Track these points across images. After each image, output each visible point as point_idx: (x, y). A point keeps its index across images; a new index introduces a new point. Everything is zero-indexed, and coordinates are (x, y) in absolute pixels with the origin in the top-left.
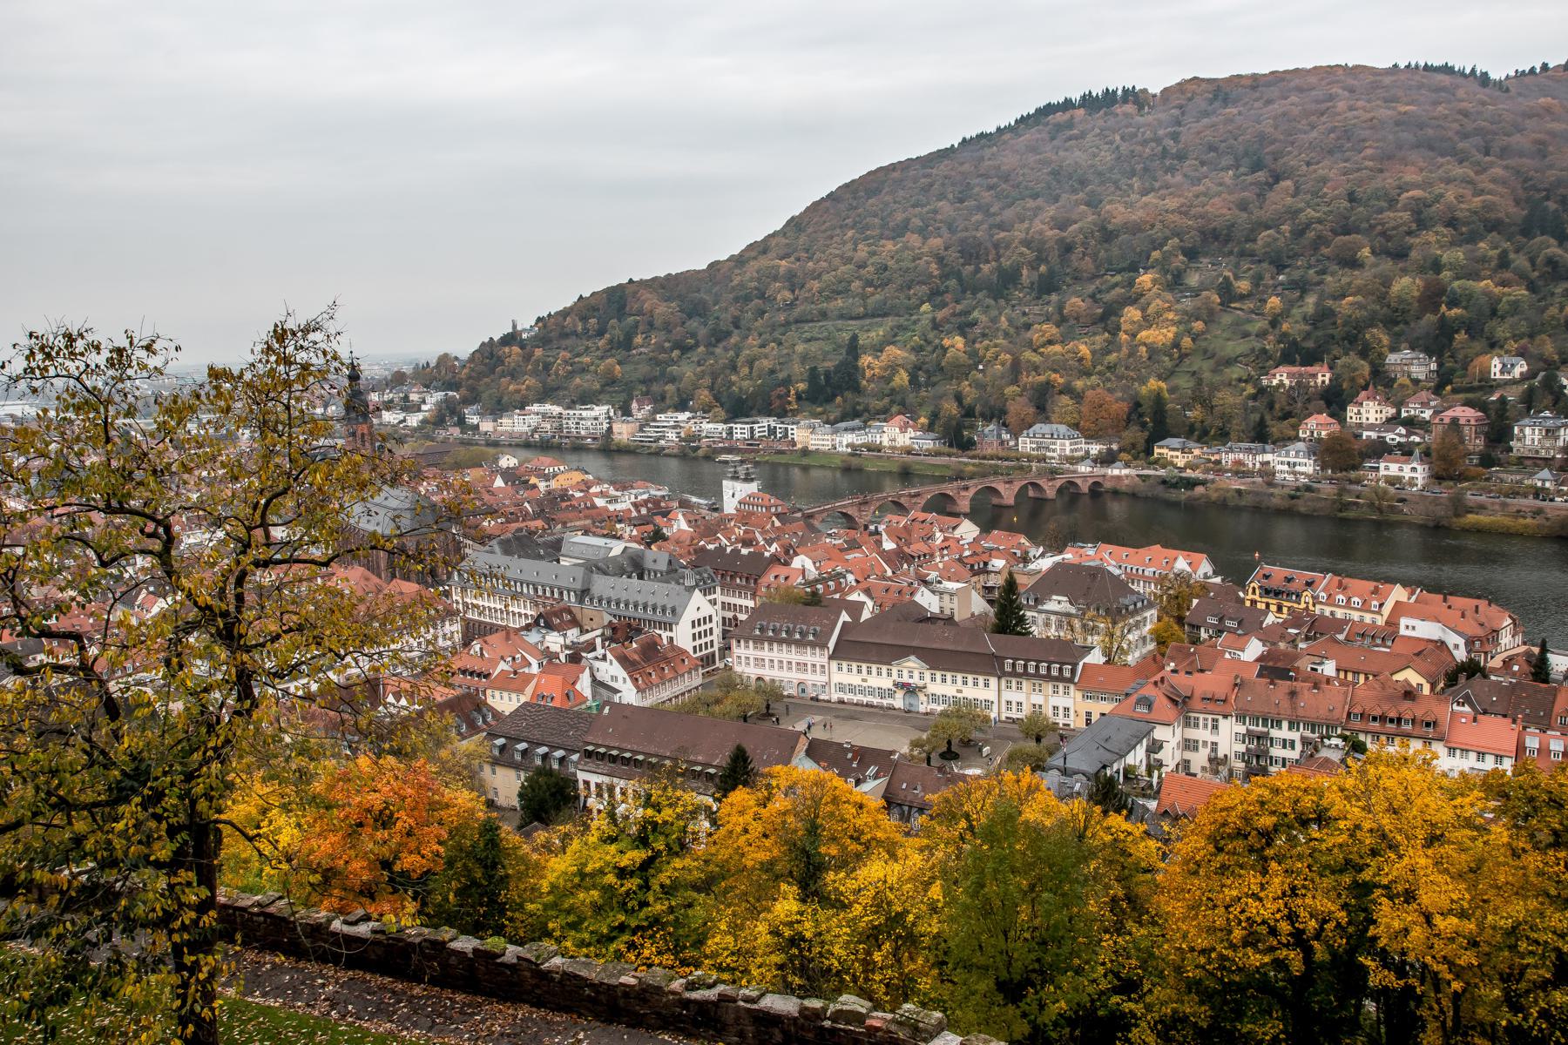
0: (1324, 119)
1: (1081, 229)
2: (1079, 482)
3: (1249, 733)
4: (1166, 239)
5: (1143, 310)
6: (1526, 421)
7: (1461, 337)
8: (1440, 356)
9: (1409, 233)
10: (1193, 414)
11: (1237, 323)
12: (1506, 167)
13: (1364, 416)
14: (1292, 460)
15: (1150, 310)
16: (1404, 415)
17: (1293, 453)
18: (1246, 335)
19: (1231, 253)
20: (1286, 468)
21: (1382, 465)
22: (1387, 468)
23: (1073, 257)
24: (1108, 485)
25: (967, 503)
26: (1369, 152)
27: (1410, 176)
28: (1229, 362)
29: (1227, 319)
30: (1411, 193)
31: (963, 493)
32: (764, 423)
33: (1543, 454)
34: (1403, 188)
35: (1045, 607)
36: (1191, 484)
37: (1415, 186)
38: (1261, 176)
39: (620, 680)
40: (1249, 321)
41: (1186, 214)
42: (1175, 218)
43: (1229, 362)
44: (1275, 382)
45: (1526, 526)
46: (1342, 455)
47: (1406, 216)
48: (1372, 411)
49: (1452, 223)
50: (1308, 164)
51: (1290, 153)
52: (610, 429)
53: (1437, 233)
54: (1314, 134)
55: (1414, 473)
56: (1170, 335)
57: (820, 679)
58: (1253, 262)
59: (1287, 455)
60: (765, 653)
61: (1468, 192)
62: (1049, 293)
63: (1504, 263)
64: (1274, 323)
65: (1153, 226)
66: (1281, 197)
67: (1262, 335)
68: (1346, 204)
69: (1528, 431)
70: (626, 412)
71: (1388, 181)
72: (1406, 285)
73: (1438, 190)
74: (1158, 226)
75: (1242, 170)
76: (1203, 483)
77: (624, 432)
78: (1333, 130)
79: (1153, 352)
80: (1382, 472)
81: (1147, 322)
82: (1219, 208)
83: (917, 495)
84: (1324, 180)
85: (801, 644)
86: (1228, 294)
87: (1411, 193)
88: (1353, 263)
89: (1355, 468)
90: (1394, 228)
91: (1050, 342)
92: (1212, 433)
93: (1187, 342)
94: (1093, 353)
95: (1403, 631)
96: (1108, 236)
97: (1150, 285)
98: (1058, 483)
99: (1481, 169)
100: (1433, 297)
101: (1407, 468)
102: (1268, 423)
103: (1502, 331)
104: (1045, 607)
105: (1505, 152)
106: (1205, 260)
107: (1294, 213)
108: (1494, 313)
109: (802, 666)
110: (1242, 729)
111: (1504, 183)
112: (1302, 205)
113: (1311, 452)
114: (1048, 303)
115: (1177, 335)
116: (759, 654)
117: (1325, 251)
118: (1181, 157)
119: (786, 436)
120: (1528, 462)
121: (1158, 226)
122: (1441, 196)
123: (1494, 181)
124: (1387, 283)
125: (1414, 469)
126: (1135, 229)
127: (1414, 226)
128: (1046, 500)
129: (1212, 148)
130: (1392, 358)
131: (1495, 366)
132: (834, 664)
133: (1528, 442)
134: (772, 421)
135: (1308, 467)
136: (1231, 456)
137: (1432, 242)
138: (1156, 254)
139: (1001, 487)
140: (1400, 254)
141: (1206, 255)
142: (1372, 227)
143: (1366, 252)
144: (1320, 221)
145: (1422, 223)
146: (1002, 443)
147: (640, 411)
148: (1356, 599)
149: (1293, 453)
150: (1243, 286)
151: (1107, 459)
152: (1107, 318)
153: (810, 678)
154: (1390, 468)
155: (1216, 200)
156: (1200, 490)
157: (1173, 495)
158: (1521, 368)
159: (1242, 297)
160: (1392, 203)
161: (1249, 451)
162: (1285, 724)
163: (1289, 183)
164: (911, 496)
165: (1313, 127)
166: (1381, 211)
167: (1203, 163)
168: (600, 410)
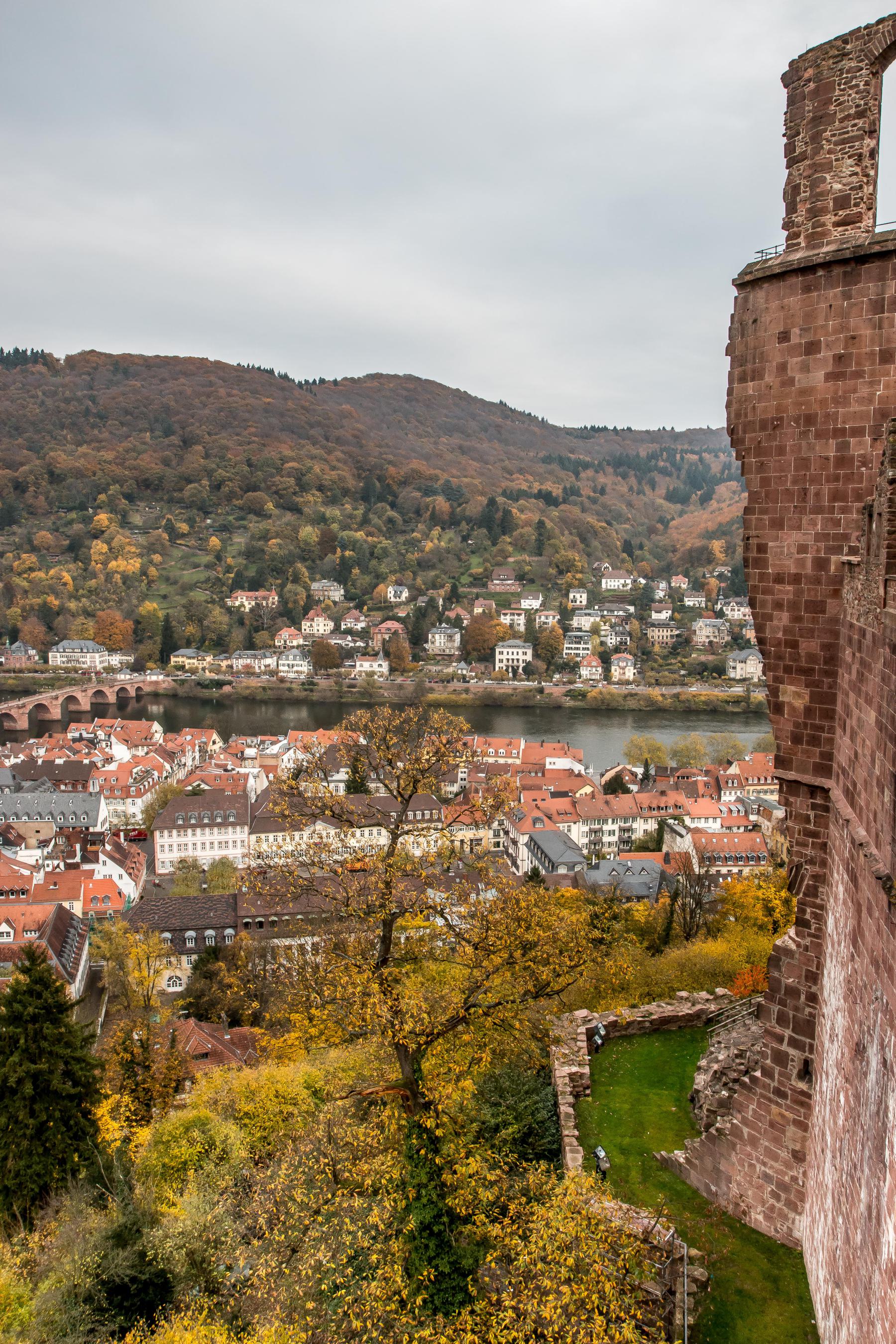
0: (211, 400)
1: (31, 472)
2: (128, 687)
3: (591, 830)
4: (108, 485)
5: (108, 543)
6: (434, 630)
7: (356, 571)
8: (345, 585)
9: (295, 493)
10: (191, 629)
11: (185, 558)
12: (342, 452)
13: (315, 628)
14: (291, 663)
15: (115, 543)
16: (343, 627)
17: (291, 657)
18: (196, 566)
19: (162, 499)
20: (286, 668)
21: (358, 664)
22: (361, 666)
23: (27, 495)
24: (147, 689)
25: (59, 710)
26: (253, 430)
27: (287, 453)
28: (193, 586)
29: (177, 553)
30: (291, 464)
31: (54, 702)
33: (447, 652)
34: (284, 460)
35: (334, 778)
36: (219, 684)
37: (293, 459)
38: (175, 439)
40: (194, 555)
41: (122, 464)
42: (114, 467)
43: (193, 586)
44: (237, 603)
45: (466, 700)
46: (323, 656)
47: (292, 481)
48: (322, 625)
49: (320, 488)
50: (209, 434)
51: (193, 424)
53: (313, 495)
54: (207, 411)
55: (381, 667)
56: (138, 565)
58: (182, 508)
59: (287, 659)
60: (189, 838)
61: (327, 468)
62: (10, 525)
63: (365, 522)
64: (219, 558)
65: (94, 475)
66: (195, 459)
67: (208, 566)
68: (246, 468)
69: (437, 636)
71: (270, 453)
72: (309, 533)
73: (309, 463)
74: (99, 473)
75: (157, 433)
76: (229, 683)
78: (221, 410)
79: (126, 578)
80: (358, 668)
81: (114, 553)
82: (150, 463)
83: (24, 706)
84: (227, 448)
85: (224, 824)
86: (174, 534)
87: (291, 464)
88: (261, 514)
89: (338, 666)
90: (284, 489)
91: (31, 569)
92: (220, 645)
93: (153, 571)
94: (74, 579)
95: (548, 767)
96: (55, 477)
97: (106, 523)
98: (116, 689)
99: (329, 452)
100: (328, 542)
101: (375, 665)
102: (255, 633)
103: (383, 569)
104: (334, 778)
105: (339, 440)
106: (142, 504)
107: (209, 473)
108: (372, 554)
109: (224, 844)
110: (586, 829)
111: (345, 463)
112: (214, 466)
113: (304, 656)
114: (14, 534)
115: (142, 565)
116: (183, 840)
117: (237, 502)
118: (102, 417)
120: (439, 658)
121: (99, 473)
122: (311, 468)
123: (338, 460)
124: (296, 530)
125: (380, 665)
126: (79, 474)
127: (297, 489)
128: (108, 704)
129: (127, 412)
130: (315, 586)
131: (390, 592)
132: (253, 837)
133: (437, 644)
135: (304, 667)
136: (241, 662)
137: (312, 500)
138: (102, 497)
139: (79, 695)
140: (296, 510)
141: (141, 499)
142: (269, 488)
143: (270, 505)
144: (230, 480)
145: (303, 487)
146: (29, 658)
148: (501, 751)
149: (291, 657)
150: (184, 527)
151: (138, 667)
152: (75, 549)
154: (364, 666)
155: (144, 456)
156: (227, 689)
157: (206, 693)
158: (405, 594)
159: (183, 536)
160: (279, 470)
161: (255, 657)
162: (610, 821)
163: (200, 448)
164: (19, 708)
165: (205, 406)
166: (272, 476)
167: (122, 424)
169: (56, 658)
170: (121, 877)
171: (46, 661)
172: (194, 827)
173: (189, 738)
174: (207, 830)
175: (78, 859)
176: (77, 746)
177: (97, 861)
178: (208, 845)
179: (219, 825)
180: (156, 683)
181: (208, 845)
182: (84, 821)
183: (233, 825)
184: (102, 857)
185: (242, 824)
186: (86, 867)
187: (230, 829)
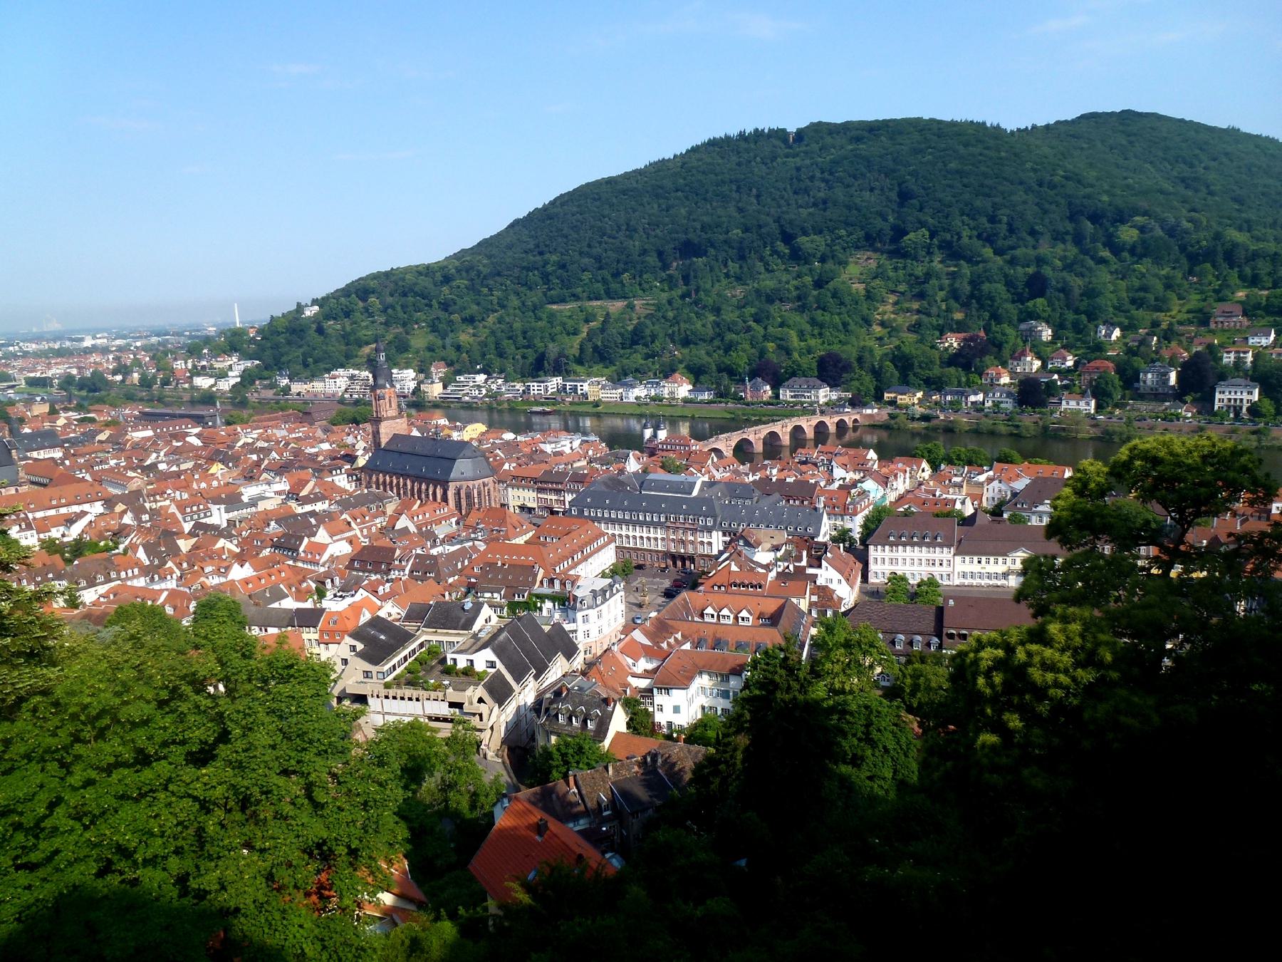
32: (555, 383)
39: (835, 581)
52: (417, 391)
57: (945, 569)
60: (900, 553)
70: (428, 376)
77: (435, 390)
101: (1082, 403)
116: (894, 555)
119: (575, 389)
132: (958, 559)
134: (559, 380)
147: (439, 371)
151: (855, 403)
153: (937, 571)
154: (1070, 404)
168: (410, 373)
169: (786, 394)
170: (840, 581)
171: (777, 396)
172: (905, 545)
173: (900, 465)
174: (916, 548)
175: (804, 563)
176: (803, 468)
177: (820, 566)
178: (916, 562)
179: (928, 545)
180: (871, 416)
181: (916, 562)
182: (811, 530)
183: (941, 546)
184: (824, 563)
185: (949, 546)
186: (810, 571)
187: (938, 549)
